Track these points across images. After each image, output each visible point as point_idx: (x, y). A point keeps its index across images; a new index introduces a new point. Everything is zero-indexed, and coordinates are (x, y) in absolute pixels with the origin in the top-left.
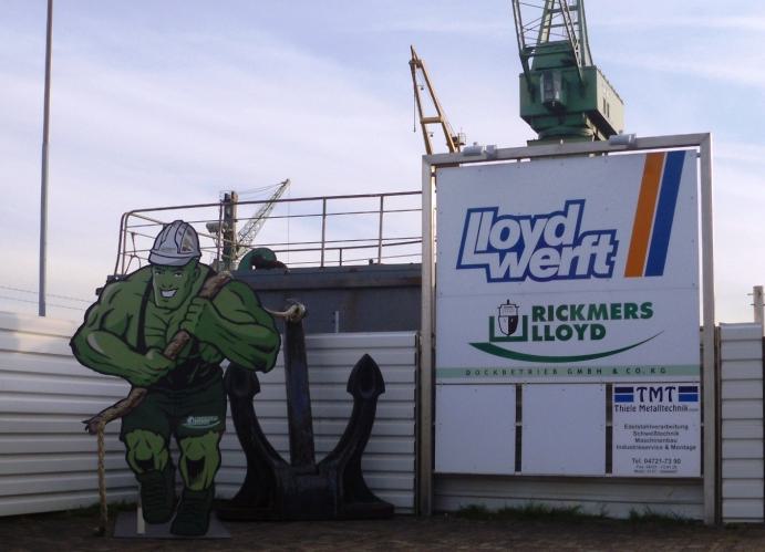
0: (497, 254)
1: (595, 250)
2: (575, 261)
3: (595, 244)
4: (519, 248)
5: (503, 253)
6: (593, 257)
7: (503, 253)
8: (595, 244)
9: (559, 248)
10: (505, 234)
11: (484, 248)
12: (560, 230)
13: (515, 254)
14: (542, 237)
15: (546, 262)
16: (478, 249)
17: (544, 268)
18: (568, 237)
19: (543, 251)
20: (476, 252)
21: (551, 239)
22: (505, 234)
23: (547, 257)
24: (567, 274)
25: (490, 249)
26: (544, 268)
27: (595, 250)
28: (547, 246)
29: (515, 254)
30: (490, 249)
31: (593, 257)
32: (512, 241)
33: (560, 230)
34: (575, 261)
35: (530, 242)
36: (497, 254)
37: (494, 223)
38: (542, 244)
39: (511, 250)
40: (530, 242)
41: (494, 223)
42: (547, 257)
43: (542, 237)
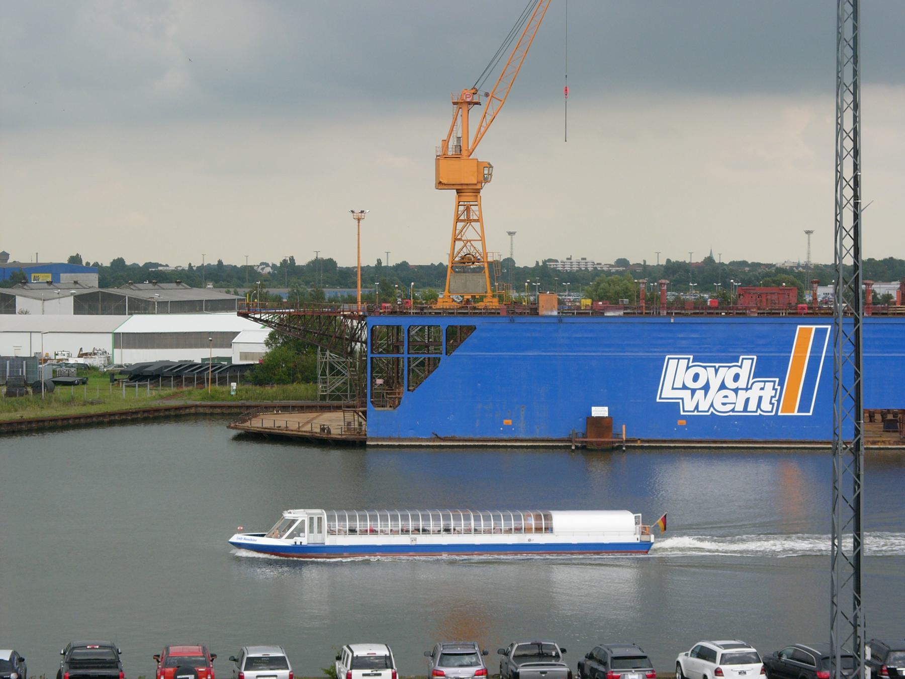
0: (690, 391)
1: (761, 393)
2: (747, 400)
3: (762, 389)
4: (706, 388)
5: (693, 391)
6: (760, 398)
7: (693, 391)
8: (762, 389)
9: (736, 391)
10: (696, 377)
12: (736, 378)
14: (723, 381)
15: (726, 400)
16: (674, 387)
17: (724, 404)
18: (742, 383)
20: (673, 388)
21: (730, 383)
22: (696, 377)
23: (726, 397)
24: (742, 410)
25: (685, 387)
26: (724, 404)
27: (761, 393)
28: (727, 388)
30: (685, 387)
31: (760, 398)
32: (701, 383)
33: (736, 378)
34: (747, 400)
35: (715, 384)
36: (690, 391)
37: (688, 368)
38: (723, 386)
40: (715, 384)
41: (688, 368)
42: (726, 397)
43: (723, 381)
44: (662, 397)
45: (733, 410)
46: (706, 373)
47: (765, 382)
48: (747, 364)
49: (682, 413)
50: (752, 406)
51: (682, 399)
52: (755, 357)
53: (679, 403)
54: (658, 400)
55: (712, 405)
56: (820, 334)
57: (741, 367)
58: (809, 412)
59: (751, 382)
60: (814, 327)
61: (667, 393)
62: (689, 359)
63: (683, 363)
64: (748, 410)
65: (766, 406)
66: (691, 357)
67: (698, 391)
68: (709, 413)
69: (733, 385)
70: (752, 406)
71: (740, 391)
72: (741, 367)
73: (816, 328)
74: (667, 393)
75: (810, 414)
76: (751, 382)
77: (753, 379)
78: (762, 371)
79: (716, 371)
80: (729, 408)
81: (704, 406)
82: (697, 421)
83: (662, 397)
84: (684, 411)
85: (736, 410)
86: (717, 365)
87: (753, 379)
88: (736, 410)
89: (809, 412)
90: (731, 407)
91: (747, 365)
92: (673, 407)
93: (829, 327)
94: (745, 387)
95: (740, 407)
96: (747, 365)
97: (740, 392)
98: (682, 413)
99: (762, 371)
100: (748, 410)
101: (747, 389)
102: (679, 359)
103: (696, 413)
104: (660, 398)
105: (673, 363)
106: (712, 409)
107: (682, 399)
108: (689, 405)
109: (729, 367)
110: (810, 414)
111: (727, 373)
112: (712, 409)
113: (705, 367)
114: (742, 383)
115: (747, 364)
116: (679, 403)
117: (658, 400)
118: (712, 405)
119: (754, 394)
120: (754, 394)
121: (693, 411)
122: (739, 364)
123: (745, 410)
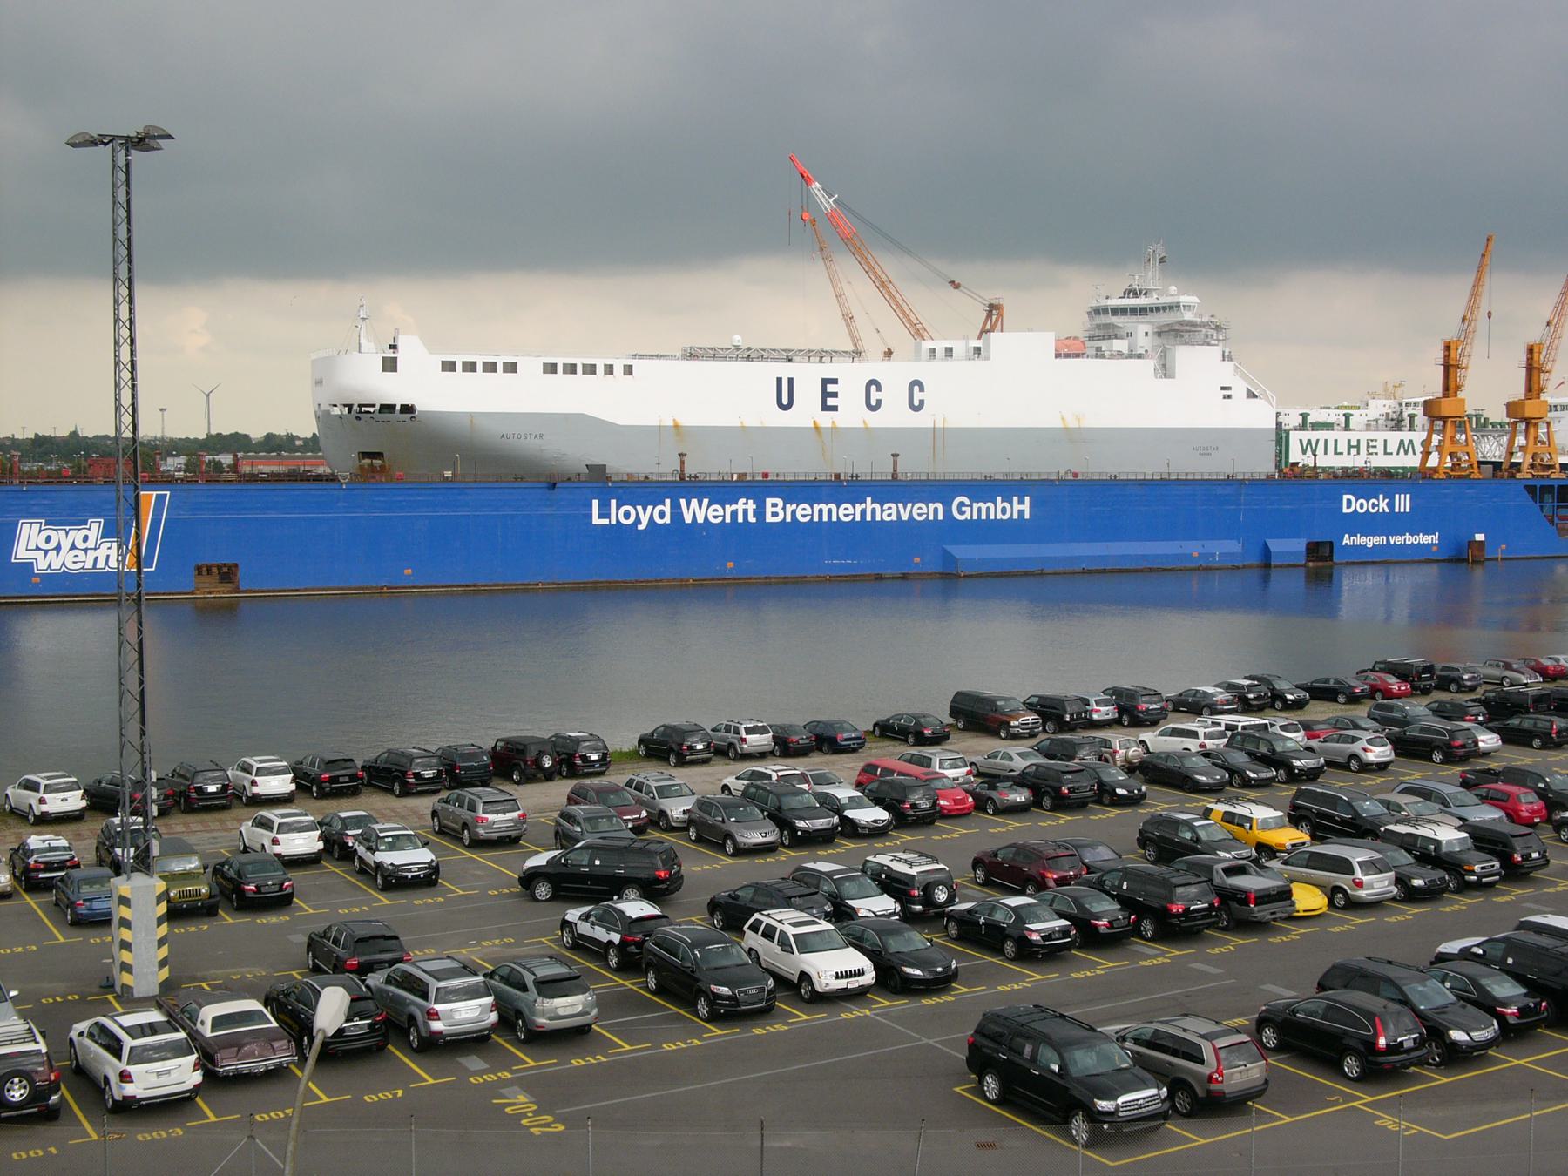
0: (43, 552)
1: (109, 552)
2: (96, 558)
3: (109, 548)
4: (58, 548)
5: (46, 552)
6: (108, 556)
7: (46, 552)
8: (109, 548)
9: (85, 550)
10: (48, 539)
11: (34, 548)
12: (86, 539)
13: (55, 552)
14: (73, 544)
15: (76, 559)
17: (74, 562)
18: (90, 543)
19: (74, 552)
20: (27, 550)
22: (48, 539)
23: (76, 556)
25: (38, 548)
26: (74, 562)
27: (109, 552)
29: (55, 552)
30: (38, 548)
31: (108, 556)
32: (53, 544)
33: (86, 539)
34: (96, 558)
35: (66, 545)
36: (43, 552)
37: (40, 531)
38: (73, 547)
39: (52, 549)
40: (66, 545)
41: (40, 531)
42: (76, 556)
43: (73, 544)
44: (17, 557)
45: (83, 568)
46: (58, 535)
47: (112, 542)
48: (95, 526)
49: (36, 572)
50: (101, 564)
51: (36, 559)
52: (102, 520)
53: (32, 563)
54: (13, 561)
55: (64, 564)
56: (160, 499)
57: (89, 529)
58: (152, 567)
59: (99, 542)
60: (155, 493)
61: (21, 553)
62: (41, 523)
63: (36, 527)
64: (98, 567)
65: (113, 563)
66: (43, 521)
67: (50, 552)
68: (61, 571)
69: (84, 546)
70: (101, 564)
71: (89, 551)
72: (89, 529)
73: (157, 495)
74: (21, 553)
75: (153, 569)
76: (99, 542)
77: (101, 538)
78: (106, 533)
79: (67, 533)
80: (80, 565)
81: (56, 565)
82: (50, 578)
83: (17, 557)
84: (38, 570)
85: (86, 567)
86: (68, 528)
87: (101, 538)
88: (86, 567)
89: (152, 567)
90: (81, 565)
91: (95, 527)
92: (28, 567)
93: (168, 493)
94: (93, 547)
95: (89, 565)
96: (95, 527)
97: (89, 551)
98: (36, 572)
99: (106, 533)
100: (98, 567)
101: (95, 549)
102: (32, 523)
103: (49, 571)
104: (15, 559)
105: (26, 527)
106: (64, 567)
107: (36, 559)
108: (42, 565)
109: (79, 530)
110: (153, 569)
111: (77, 535)
112: (64, 567)
113: (56, 530)
114: (90, 543)
115: (95, 526)
116: (32, 563)
117: (13, 561)
118: (64, 564)
119: (102, 553)
120: (102, 553)
121: (46, 570)
122: (88, 527)
123: (94, 567)
